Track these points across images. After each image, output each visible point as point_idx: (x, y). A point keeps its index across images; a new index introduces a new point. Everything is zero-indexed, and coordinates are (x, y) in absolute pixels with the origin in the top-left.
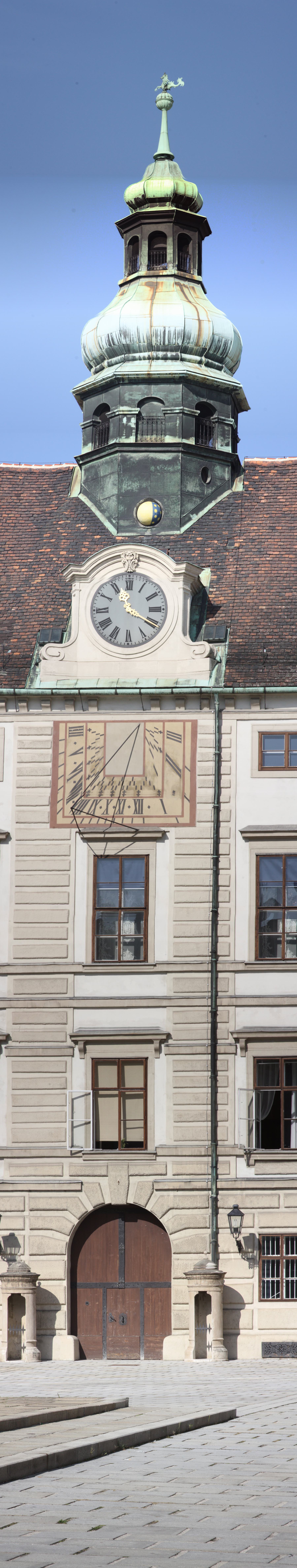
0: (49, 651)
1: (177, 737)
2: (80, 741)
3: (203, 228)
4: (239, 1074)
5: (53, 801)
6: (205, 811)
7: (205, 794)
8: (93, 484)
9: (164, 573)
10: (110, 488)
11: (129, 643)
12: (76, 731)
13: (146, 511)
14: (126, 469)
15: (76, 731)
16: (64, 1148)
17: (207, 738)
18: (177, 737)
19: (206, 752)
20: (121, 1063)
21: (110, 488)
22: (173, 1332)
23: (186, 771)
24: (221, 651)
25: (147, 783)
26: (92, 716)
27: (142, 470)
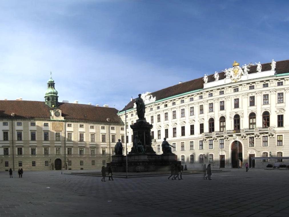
1: (62, 124)
2: (54, 124)
3: (54, 83)
4: (67, 149)
5: (53, 128)
6: (64, 129)
7: (64, 128)
8: (48, 103)
9: (60, 111)
10: (50, 104)
11: (57, 116)
12: (54, 123)
13: (53, 106)
14: (51, 103)
16: (77, 155)
18: (62, 124)
19: (64, 125)
20: (82, 148)
22: (62, 169)
26: (55, 122)
27: (53, 103)
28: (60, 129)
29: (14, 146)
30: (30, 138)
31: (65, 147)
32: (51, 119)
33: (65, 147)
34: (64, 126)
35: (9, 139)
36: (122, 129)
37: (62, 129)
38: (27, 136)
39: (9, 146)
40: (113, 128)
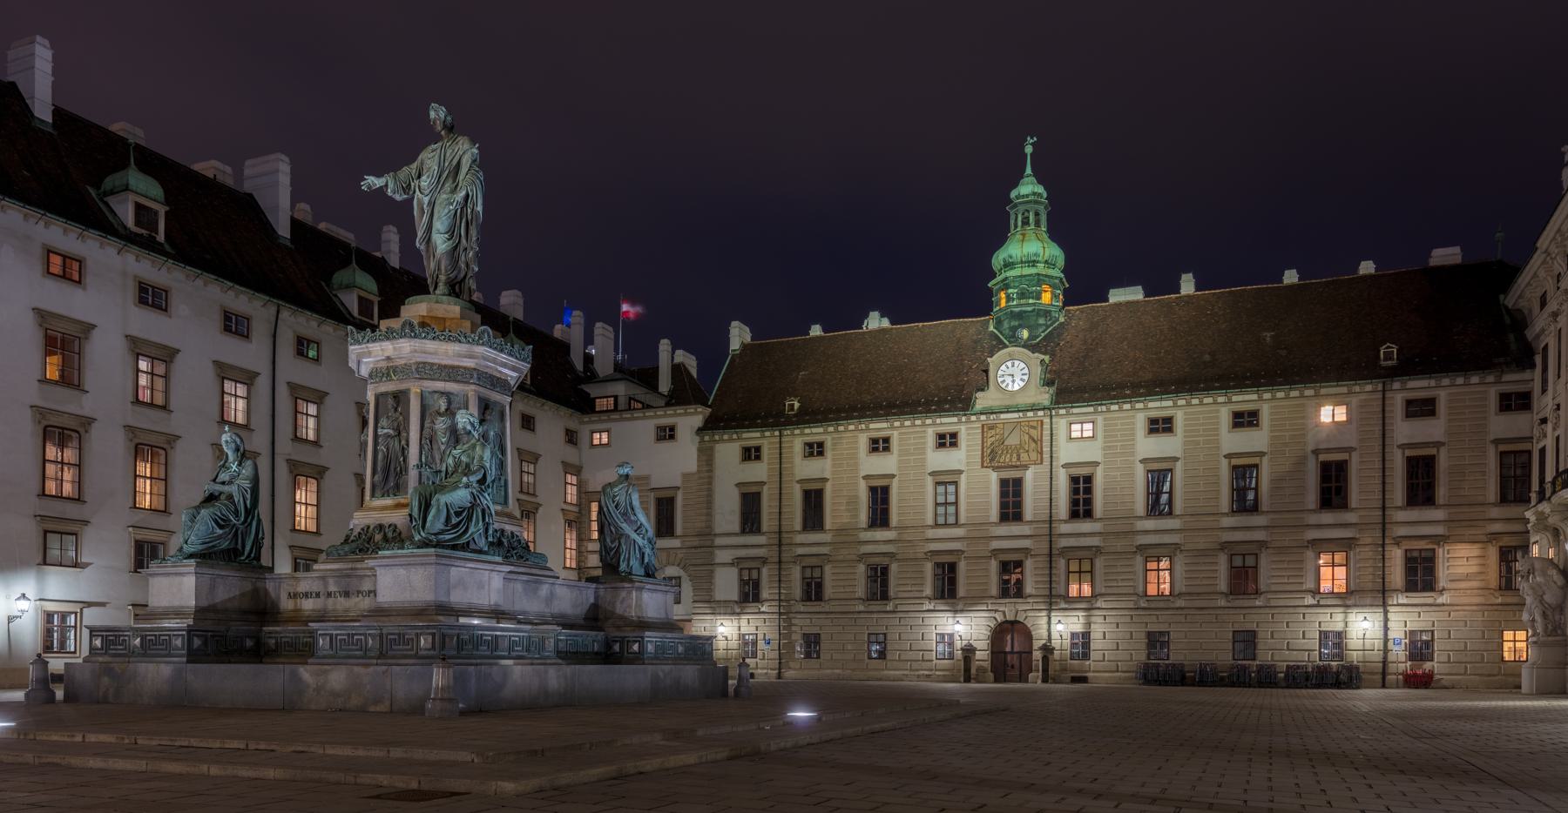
0: (979, 394)
6: (1046, 456)
7: (1046, 449)
12: (992, 428)
15: (992, 428)
17: (1047, 426)
19: (1047, 432)
21: (1006, 325)
23: (1038, 441)
24: (1052, 390)
25: (1021, 447)
27: (1020, 316)
28: (1024, 456)
29: (786, 556)
30: (863, 517)
31: (1051, 555)
32: (978, 406)
33: (1051, 555)
34: (1046, 438)
35: (765, 528)
36: (1517, 402)
37: (1034, 456)
38: (846, 507)
39: (764, 561)
40: (1422, 408)
